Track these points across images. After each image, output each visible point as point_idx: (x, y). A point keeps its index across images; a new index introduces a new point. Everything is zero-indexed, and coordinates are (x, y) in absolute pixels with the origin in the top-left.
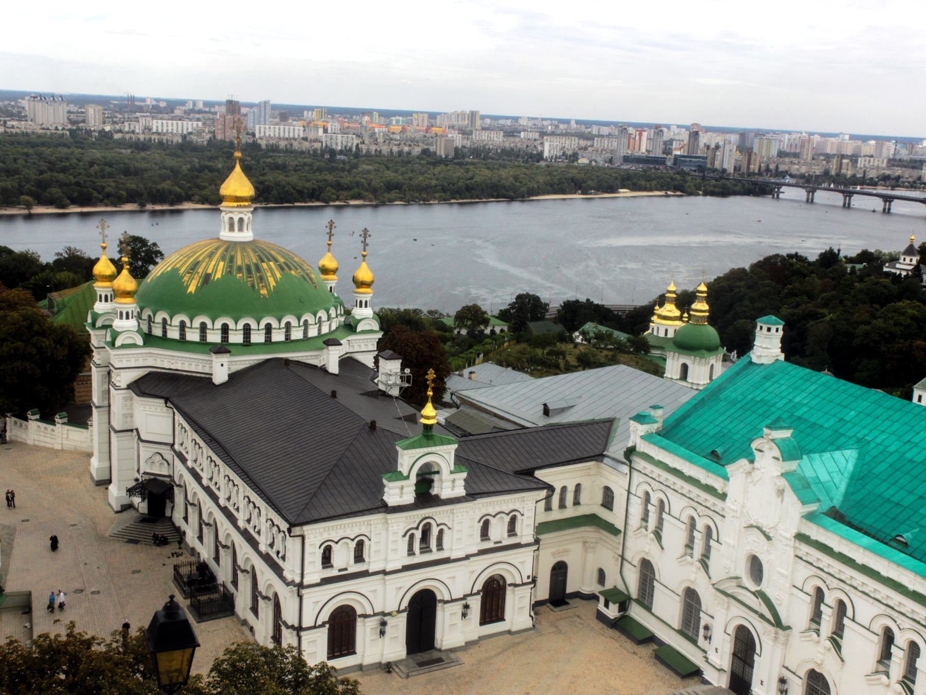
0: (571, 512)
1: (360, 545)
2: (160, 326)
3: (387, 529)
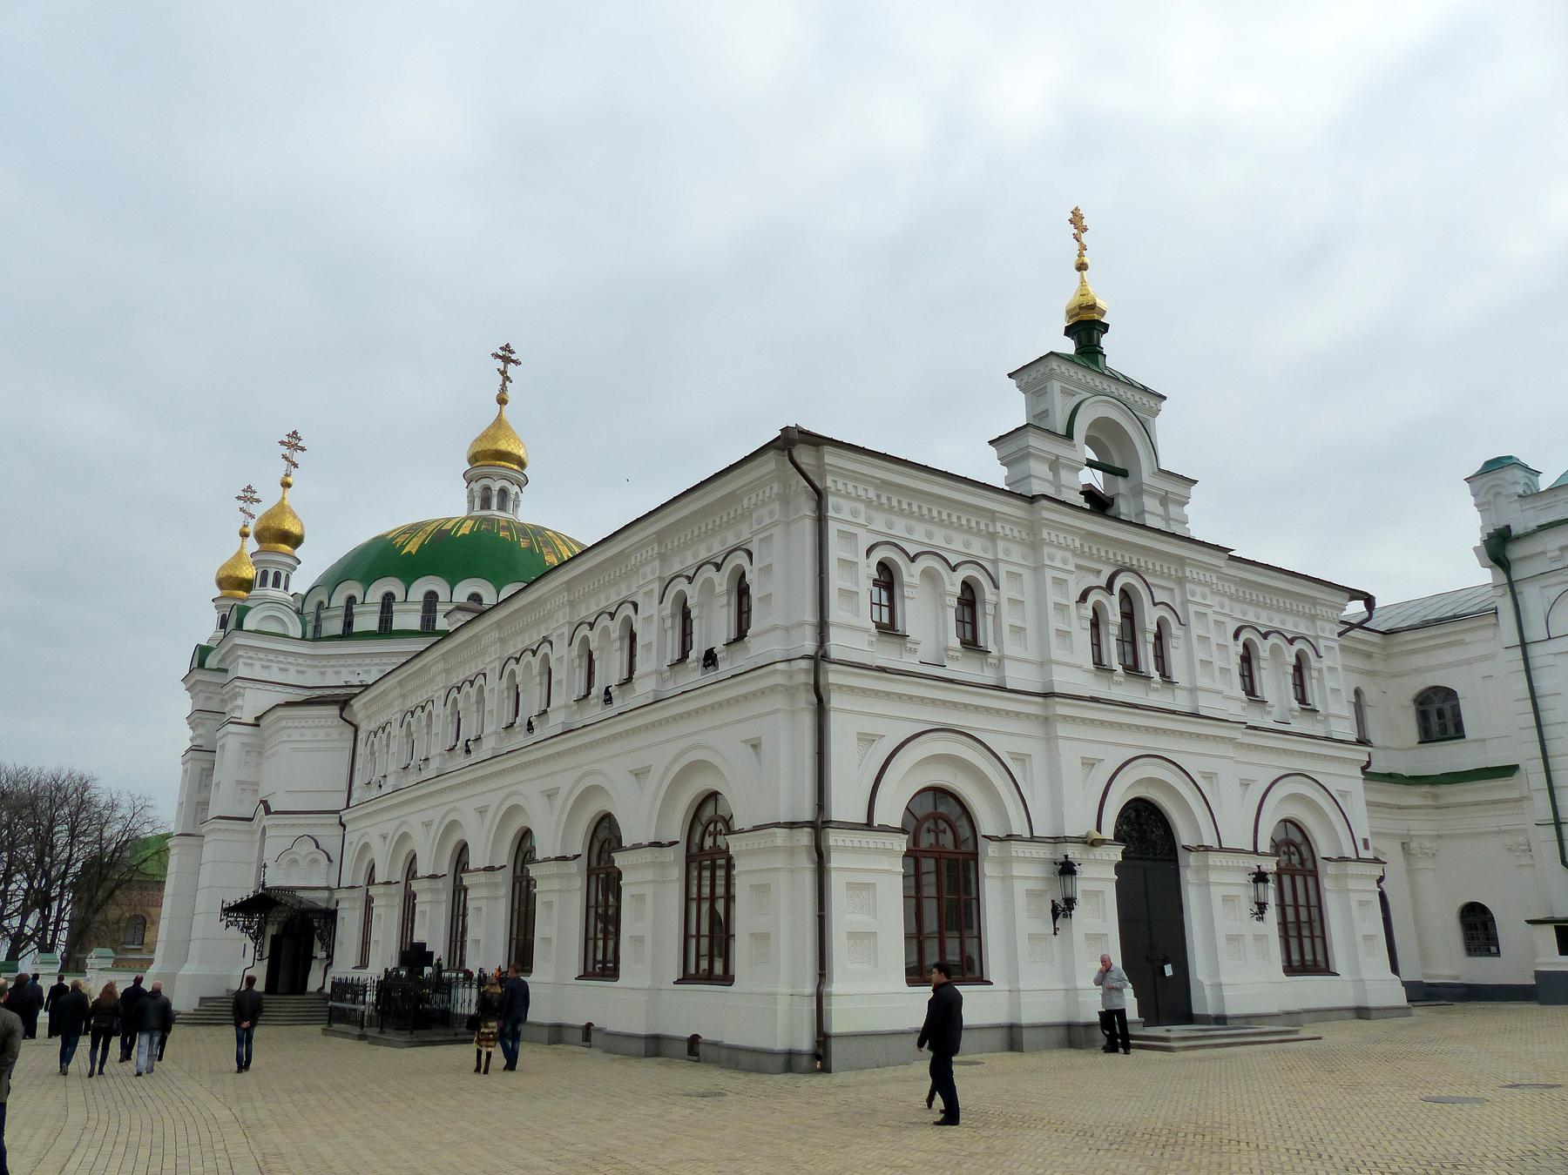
1: (969, 599)
2: (342, 612)
3: (1038, 569)
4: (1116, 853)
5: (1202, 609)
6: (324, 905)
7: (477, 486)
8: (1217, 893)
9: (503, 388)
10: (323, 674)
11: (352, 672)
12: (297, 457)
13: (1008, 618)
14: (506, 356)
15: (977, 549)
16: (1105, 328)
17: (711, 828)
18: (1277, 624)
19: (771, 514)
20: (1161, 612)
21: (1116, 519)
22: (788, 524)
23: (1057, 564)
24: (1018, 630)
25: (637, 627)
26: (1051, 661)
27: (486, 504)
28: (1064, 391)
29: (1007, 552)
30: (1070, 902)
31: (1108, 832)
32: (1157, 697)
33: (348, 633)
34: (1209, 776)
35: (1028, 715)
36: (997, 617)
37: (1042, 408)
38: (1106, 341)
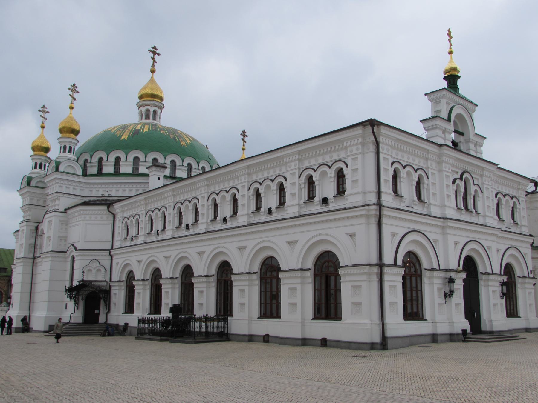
2: (97, 164)
4: (464, 275)
5: (488, 187)
6: (104, 288)
7: (143, 109)
8: (491, 289)
9: (153, 66)
10: (91, 191)
11: (104, 191)
12: (76, 95)
13: (431, 191)
14: (154, 51)
15: (422, 164)
16: (459, 77)
17: (326, 264)
18: (507, 192)
19: (357, 149)
20: (476, 187)
21: (460, 151)
22: (364, 154)
23: (447, 170)
24: (434, 194)
25: (286, 185)
26: (445, 206)
27: (148, 117)
28: (448, 104)
29: (431, 165)
30: (452, 292)
31: (461, 268)
32: (474, 219)
33: (100, 173)
34: (489, 248)
35: (438, 226)
36: (428, 189)
37: (437, 109)
38: (459, 82)
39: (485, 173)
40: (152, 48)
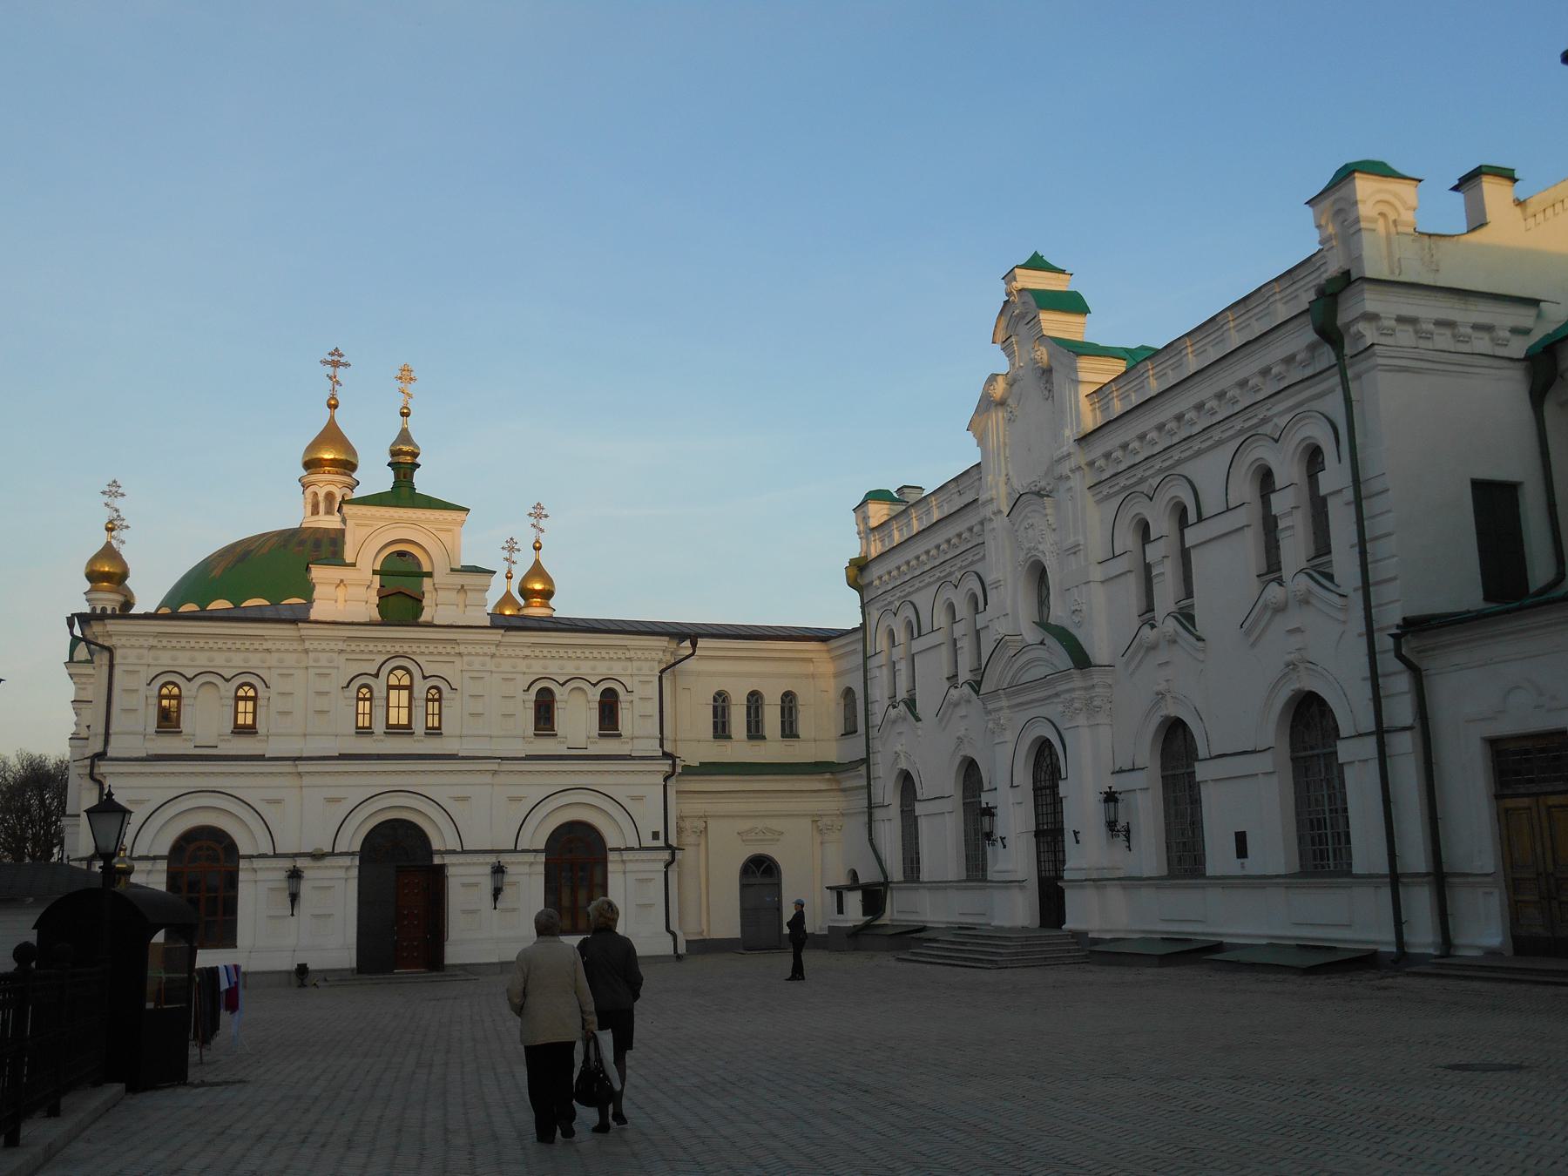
0: (773, 749)
39: (462, 649)
40: (331, 354)
